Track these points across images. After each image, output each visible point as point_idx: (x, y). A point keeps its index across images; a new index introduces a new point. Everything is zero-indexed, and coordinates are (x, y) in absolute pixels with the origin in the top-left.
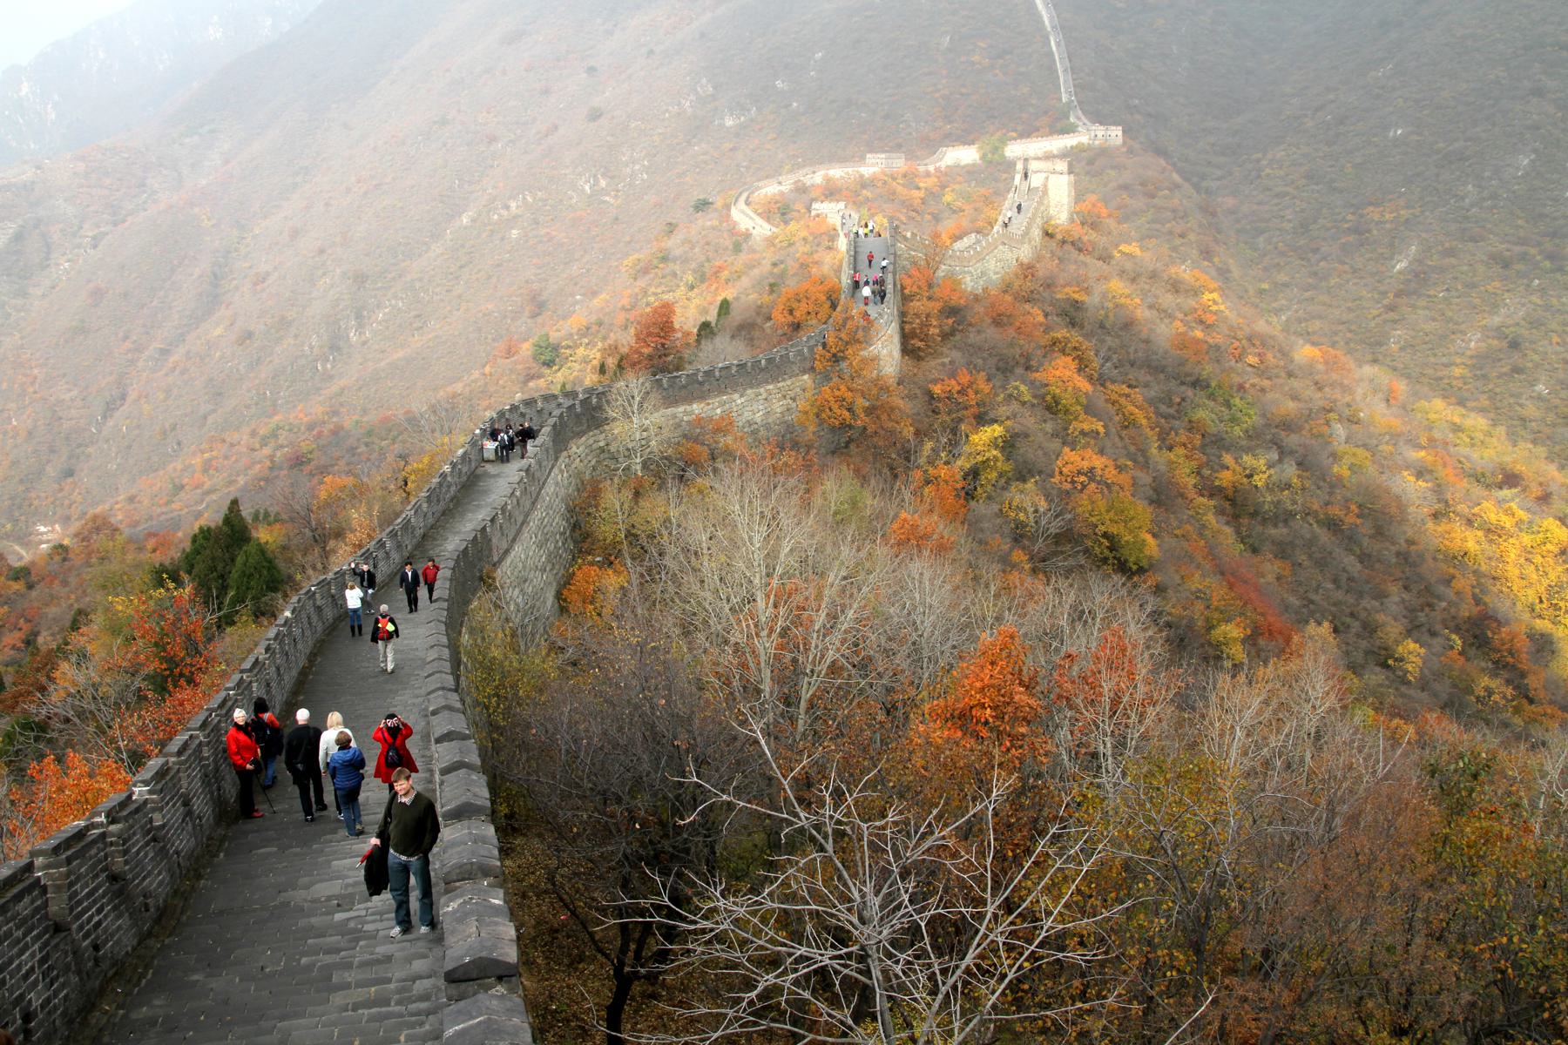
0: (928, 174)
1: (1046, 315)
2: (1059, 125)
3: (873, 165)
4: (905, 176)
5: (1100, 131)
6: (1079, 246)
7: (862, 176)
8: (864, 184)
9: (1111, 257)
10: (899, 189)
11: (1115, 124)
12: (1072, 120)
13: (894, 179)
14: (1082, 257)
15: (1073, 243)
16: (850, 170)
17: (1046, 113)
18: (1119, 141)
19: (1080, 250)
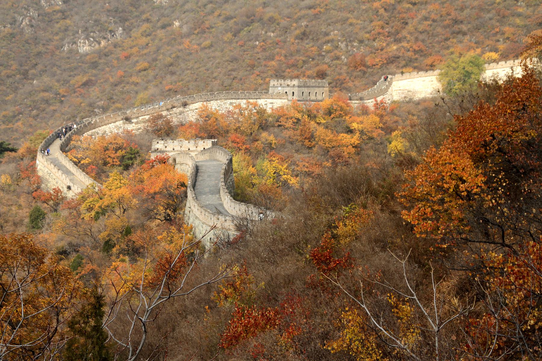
0: (365, 111)
3: (279, 96)
4: (329, 112)
7: (261, 112)
8: (264, 123)
13: (312, 116)
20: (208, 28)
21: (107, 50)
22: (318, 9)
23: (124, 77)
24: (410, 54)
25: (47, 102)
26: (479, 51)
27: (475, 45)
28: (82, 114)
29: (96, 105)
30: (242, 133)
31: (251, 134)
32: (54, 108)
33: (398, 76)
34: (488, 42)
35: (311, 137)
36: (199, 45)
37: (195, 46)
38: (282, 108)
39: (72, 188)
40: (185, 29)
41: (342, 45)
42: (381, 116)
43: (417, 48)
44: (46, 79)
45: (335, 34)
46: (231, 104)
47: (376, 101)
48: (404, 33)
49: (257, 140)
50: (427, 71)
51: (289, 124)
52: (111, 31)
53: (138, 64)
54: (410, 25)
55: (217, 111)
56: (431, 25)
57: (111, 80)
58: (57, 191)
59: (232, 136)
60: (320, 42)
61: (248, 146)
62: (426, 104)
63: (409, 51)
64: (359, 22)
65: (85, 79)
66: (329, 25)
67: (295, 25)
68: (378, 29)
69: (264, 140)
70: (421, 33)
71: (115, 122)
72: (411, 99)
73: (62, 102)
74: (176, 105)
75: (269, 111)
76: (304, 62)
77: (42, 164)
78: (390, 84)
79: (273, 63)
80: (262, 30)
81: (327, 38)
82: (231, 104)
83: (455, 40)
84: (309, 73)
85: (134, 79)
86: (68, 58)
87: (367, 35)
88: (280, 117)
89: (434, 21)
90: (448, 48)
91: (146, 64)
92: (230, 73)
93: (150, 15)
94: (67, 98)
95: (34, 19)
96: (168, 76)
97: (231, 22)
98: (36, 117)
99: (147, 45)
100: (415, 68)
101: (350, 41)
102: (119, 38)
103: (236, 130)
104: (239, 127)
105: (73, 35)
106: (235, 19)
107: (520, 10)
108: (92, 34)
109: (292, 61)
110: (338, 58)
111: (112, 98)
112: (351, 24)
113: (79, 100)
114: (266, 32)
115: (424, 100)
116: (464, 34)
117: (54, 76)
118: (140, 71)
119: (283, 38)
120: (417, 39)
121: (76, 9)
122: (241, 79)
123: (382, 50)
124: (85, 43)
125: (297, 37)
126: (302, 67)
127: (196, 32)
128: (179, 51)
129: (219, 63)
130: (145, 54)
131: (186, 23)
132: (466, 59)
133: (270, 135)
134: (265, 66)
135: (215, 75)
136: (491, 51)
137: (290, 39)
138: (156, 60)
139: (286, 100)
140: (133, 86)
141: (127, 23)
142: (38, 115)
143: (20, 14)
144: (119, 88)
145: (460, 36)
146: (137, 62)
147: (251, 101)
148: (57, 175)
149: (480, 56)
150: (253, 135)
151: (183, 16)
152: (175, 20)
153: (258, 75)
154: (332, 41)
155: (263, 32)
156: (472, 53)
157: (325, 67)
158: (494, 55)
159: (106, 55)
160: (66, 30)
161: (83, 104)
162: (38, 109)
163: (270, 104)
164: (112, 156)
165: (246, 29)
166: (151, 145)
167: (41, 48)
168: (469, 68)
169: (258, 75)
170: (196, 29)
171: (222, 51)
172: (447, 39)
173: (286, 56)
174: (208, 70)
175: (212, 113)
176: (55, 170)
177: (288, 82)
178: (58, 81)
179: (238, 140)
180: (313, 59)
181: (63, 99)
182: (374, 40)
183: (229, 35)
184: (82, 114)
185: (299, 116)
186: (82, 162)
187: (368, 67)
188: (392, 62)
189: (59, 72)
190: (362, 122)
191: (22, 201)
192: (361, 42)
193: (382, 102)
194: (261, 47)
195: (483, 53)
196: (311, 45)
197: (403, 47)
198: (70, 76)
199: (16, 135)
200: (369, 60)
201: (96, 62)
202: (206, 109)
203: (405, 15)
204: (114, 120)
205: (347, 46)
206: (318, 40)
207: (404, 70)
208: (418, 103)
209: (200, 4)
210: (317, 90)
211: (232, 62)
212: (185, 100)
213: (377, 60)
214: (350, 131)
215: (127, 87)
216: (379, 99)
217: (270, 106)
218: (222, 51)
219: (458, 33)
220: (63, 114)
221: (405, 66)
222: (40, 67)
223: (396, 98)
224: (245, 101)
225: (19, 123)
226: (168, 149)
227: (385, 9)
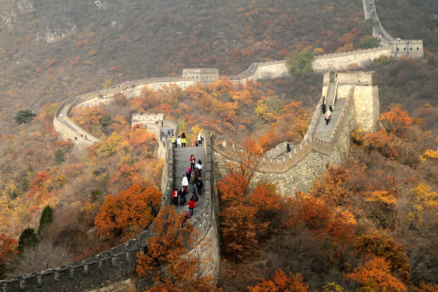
0: (241, 88)
1: (358, 217)
2: (362, 41)
3: (189, 79)
4: (219, 89)
5: (402, 45)
6: (385, 152)
7: (179, 90)
8: (181, 96)
9: (417, 162)
11: (416, 37)
12: (374, 35)
13: (209, 92)
14: (389, 163)
15: (380, 150)
16: (167, 84)
17: (350, 29)
18: (421, 53)
19: (387, 156)
21: (66, 41)
22: (209, 17)
23: (81, 60)
24: (268, 48)
25: (28, 76)
26: (311, 47)
27: (309, 43)
28: (54, 85)
29: (63, 80)
30: (169, 103)
31: (174, 104)
32: (33, 81)
33: (261, 63)
34: (317, 41)
35: (210, 105)
36: (131, 39)
37: (129, 40)
38: (190, 86)
39: (78, 138)
40: (120, 27)
41: (226, 42)
42: (251, 91)
43: (273, 45)
44: (25, 60)
45: (221, 34)
46: (160, 85)
47: (248, 80)
48: (265, 34)
49: (177, 107)
50: (279, 60)
53: (89, 51)
54: (269, 29)
55: (152, 90)
56: (282, 29)
57: (72, 62)
58: (69, 140)
59: (163, 105)
60: (211, 39)
61: (172, 111)
62: (279, 81)
63: (268, 46)
64: (236, 26)
65: (53, 61)
66: (217, 27)
67: (194, 27)
69: (181, 107)
70: (276, 34)
71: (93, 98)
73: (38, 77)
75: (184, 89)
76: (202, 53)
77: (57, 125)
78: (256, 68)
79: (182, 53)
80: (173, 29)
81: (216, 37)
82: (160, 85)
83: (297, 39)
84: (205, 60)
85: (88, 62)
86: (40, 46)
87: (242, 36)
88: (190, 93)
89: (284, 26)
90: (292, 44)
91: (95, 52)
92: (153, 59)
93: (95, 17)
94: (42, 74)
95: (14, 18)
96: (111, 60)
97: (152, 24)
98: (20, 87)
99: (94, 37)
100: (272, 58)
101: (231, 39)
102: (74, 32)
103: (164, 102)
104: (166, 100)
105: (43, 30)
106: (154, 22)
107: (338, 19)
108: (56, 29)
110: (223, 50)
111: (73, 75)
112: (231, 28)
113: (51, 76)
114: (176, 31)
115: (278, 79)
116: (303, 35)
117: (31, 58)
118: (91, 56)
119: (187, 35)
120: (273, 38)
121: (43, 12)
122: (161, 64)
123: (251, 45)
124: (51, 36)
125: (196, 36)
126: (200, 56)
127: (128, 29)
128: (118, 43)
129: (145, 52)
130: (94, 44)
131: (121, 23)
132: (303, 53)
133: (185, 104)
134: (177, 55)
135: (143, 60)
136: (319, 47)
138: (102, 48)
139: (193, 82)
140: (87, 67)
141: (79, 22)
142: (22, 86)
143: (5, 15)
144: (78, 68)
145: (300, 36)
146: (89, 49)
147: (172, 83)
148: (68, 131)
149: (312, 50)
150: (175, 104)
151: (118, 18)
152: (112, 20)
153: (172, 61)
154: (219, 38)
155: (174, 32)
156: (306, 50)
157: (215, 56)
158: (320, 50)
159: (65, 44)
160: (37, 26)
161: (54, 79)
162: (22, 81)
164: (95, 119)
165: (162, 29)
166: (131, 118)
167: (20, 39)
168: (305, 59)
169: (172, 61)
170: (128, 28)
171: (147, 44)
172: (292, 39)
173: (189, 48)
174: (138, 57)
175: (150, 91)
176: (67, 128)
177: (194, 70)
178: (34, 62)
179: (166, 108)
180: (207, 51)
181: (39, 74)
182: (246, 39)
183: (150, 34)
184: (54, 85)
185: (201, 92)
186: (80, 123)
187: (242, 57)
188: (257, 53)
189: (34, 56)
190: (239, 95)
191: (48, 146)
192: (238, 40)
193: (251, 81)
194: (173, 41)
195: (314, 48)
196: (205, 41)
197: (264, 43)
198: (42, 58)
199: (9, 99)
201: (59, 49)
202: (145, 89)
203: (265, 22)
204: (93, 97)
205: (229, 42)
206: (210, 38)
207: (265, 59)
208: (273, 81)
209: (129, 10)
210: (211, 75)
211: (154, 51)
212: (134, 83)
213: (248, 52)
214: (232, 101)
215: (84, 67)
216: (250, 78)
217: (184, 85)
218: (147, 44)
219: (299, 34)
220: (40, 85)
221: (266, 56)
222: (20, 52)
223: (260, 77)
224: (168, 83)
225: (10, 91)
226: (141, 119)
227: (253, 18)
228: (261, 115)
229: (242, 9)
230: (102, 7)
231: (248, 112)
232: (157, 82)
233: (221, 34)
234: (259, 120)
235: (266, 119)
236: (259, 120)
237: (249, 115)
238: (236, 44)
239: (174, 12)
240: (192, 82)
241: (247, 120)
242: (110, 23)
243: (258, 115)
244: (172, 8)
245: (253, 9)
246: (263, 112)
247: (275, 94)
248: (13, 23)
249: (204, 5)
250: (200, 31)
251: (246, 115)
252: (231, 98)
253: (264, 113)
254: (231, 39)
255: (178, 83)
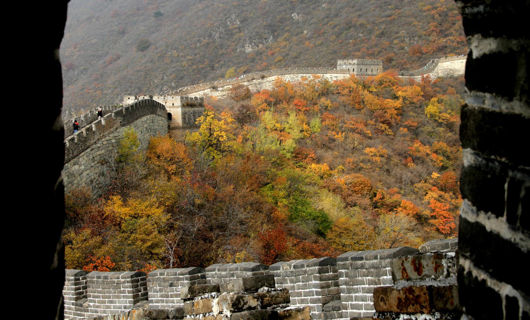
3: (342, 71)
4: (381, 83)
8: (326, 91)
10: (367, 96)
20: (322, 33)
22: (393, 17)
24: (454, 44)
41: (407, 40)
43: (459, 40)
47: (423, 76)
48: (452, 30)
51: (346, 91)
52: (265, 39)
66: (400, 27)
68: (432, 28)
72: (451, 76)
74: (255, 77)
76: (380, 52)
78: (437, 64)
81: (397, 35)
87: (425, 32)
91: (281, 58)
109: (371, 51)
110: (402, 48)
112: (414, 26)
114: (358, 34)
118: (277, 62)
135: (320, 63)
137: (373, 37)
157: (391, 55)
163: (332, 77)
180: (386, 50)
182: (429, 35)
183: (334, 37)
187: (423, 54)
192: (420, 37)
193: (427, 77)
197: (450, 40)
200: (424, 50)
205: (410, 40)
210: (373, 67)
213: (430, 49)
223: (441, 75)
228: (432, 116)
229: (429, 7)
230: (298, 20)
231: (415, 112)
232: (298, 74)
233: (403, 33)
234: (430, 122)
235: (440, 121)
236: (430, 122)
237: (416, 117)
238: (418, 41)
239: (360, 16)
240: (348, 76)
241: (413, 122)
242: (302, 32)
243: (429, 116)
244: (359, 13)
245: (441, 7)
246: (435, 112)
247: (457, 93)
248: (220, 38)
249: (390, 7)
250: (381, 31)
251: (413, 116)
252: (395, 95)
253: (438, 114)
254: (413, 37)
255: (328, 76)
